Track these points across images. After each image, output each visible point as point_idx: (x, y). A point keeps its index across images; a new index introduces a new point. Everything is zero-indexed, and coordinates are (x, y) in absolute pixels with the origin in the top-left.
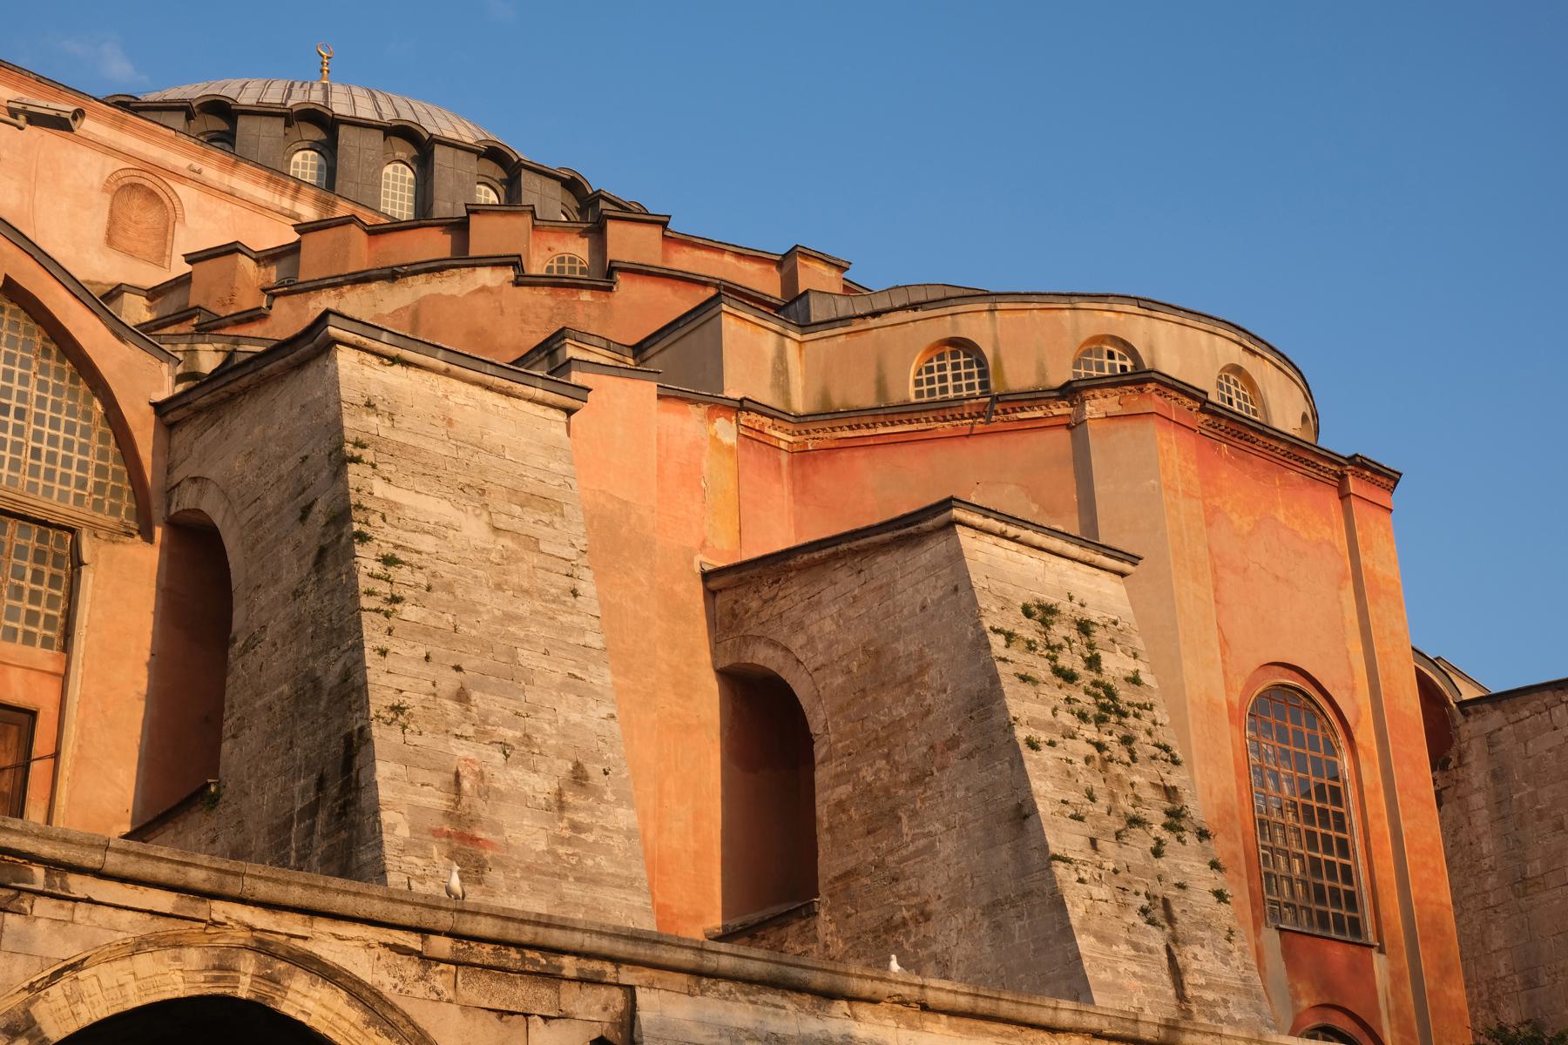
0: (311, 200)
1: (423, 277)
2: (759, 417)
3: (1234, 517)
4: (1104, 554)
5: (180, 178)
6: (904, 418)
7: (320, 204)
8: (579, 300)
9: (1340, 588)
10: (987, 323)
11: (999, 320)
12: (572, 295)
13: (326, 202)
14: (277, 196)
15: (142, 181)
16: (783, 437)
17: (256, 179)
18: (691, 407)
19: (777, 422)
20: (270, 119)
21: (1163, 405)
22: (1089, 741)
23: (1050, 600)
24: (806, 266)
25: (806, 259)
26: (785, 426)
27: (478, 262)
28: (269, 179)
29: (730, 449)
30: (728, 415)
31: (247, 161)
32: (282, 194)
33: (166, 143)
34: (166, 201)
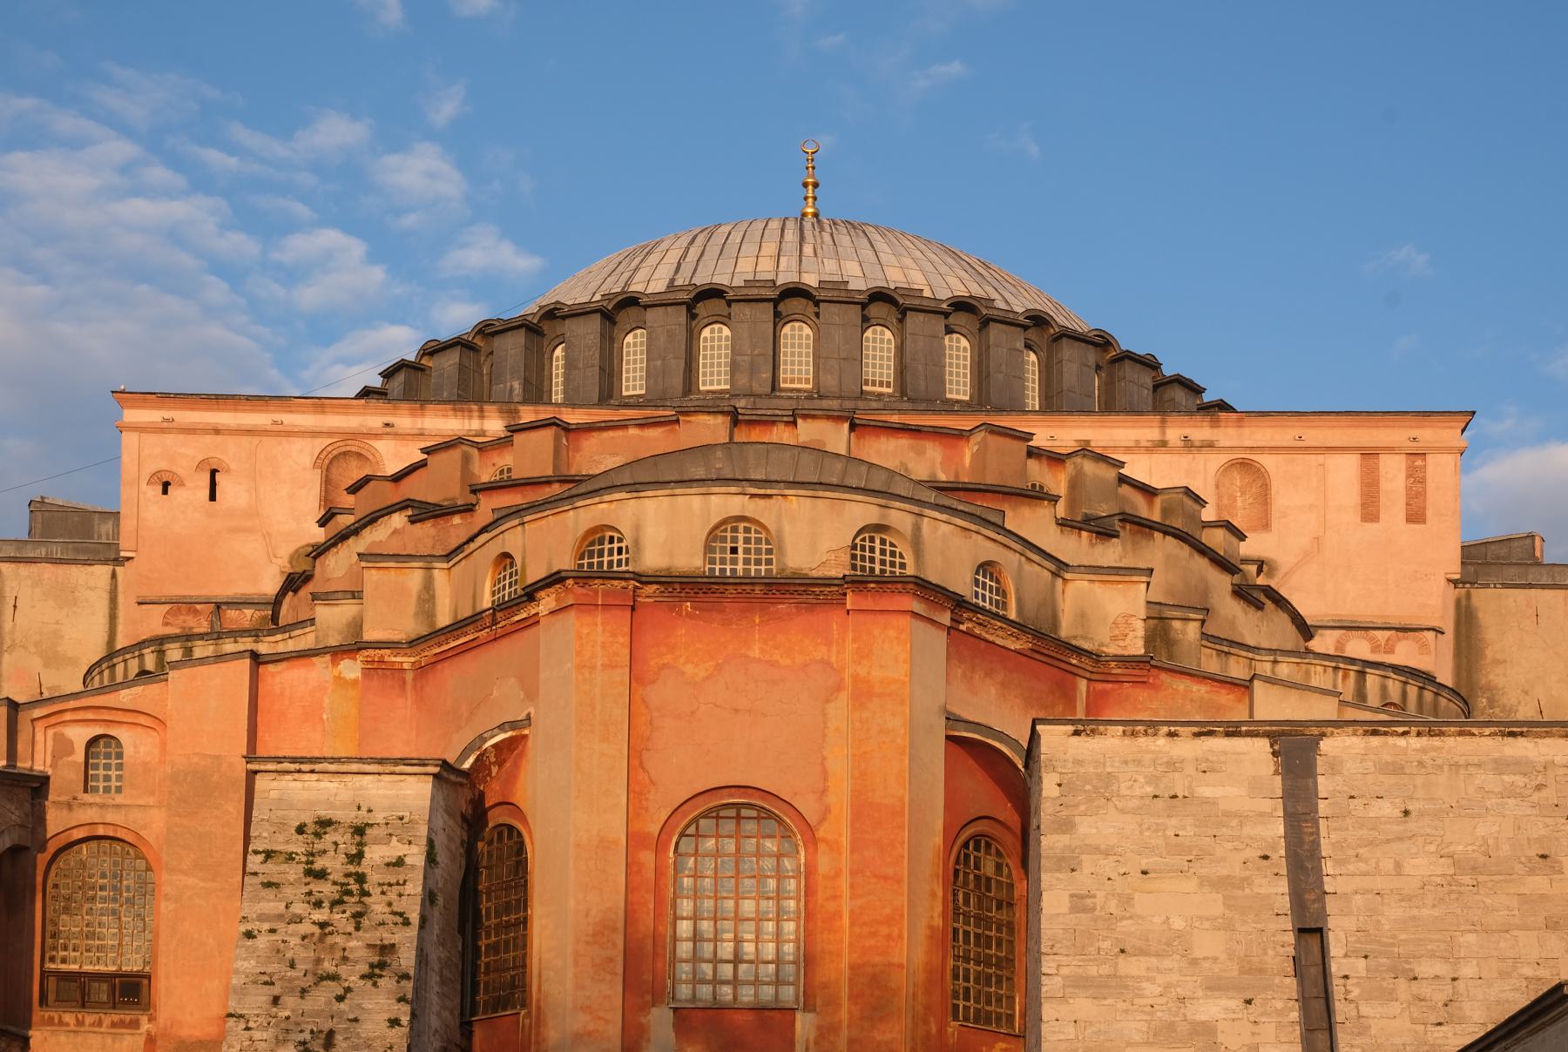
0: (498, 414)
1: (368, 529)
2: (377, 651)
3: (689, 669)
4: (405, 765)
5: (377, 436)
6: (459, 632)
7: (506, 415)
8: (452, 525)
9: (827, 701)
10: (520, 536)
11: (527, 531)
12: (448, 521)
13: (510, 412)
14: (466, 421)
15: (348, 448)
16: (406, 661)
17: (445, 413)
18: (314, 659)
19: (395, 651)
20: (515, 331)
21: (587, 594)
22: (314, 923)
23: (325, 813)
24: (689, 422)
25: (688, 415)
26: (402, 652)
27: (390, 510)
28: (455, 410)
29: (355, 682)
30: (352, 655)
31: (431, 402)
32: (470, 417)
33: (362, 411)
34: (371, 457)
